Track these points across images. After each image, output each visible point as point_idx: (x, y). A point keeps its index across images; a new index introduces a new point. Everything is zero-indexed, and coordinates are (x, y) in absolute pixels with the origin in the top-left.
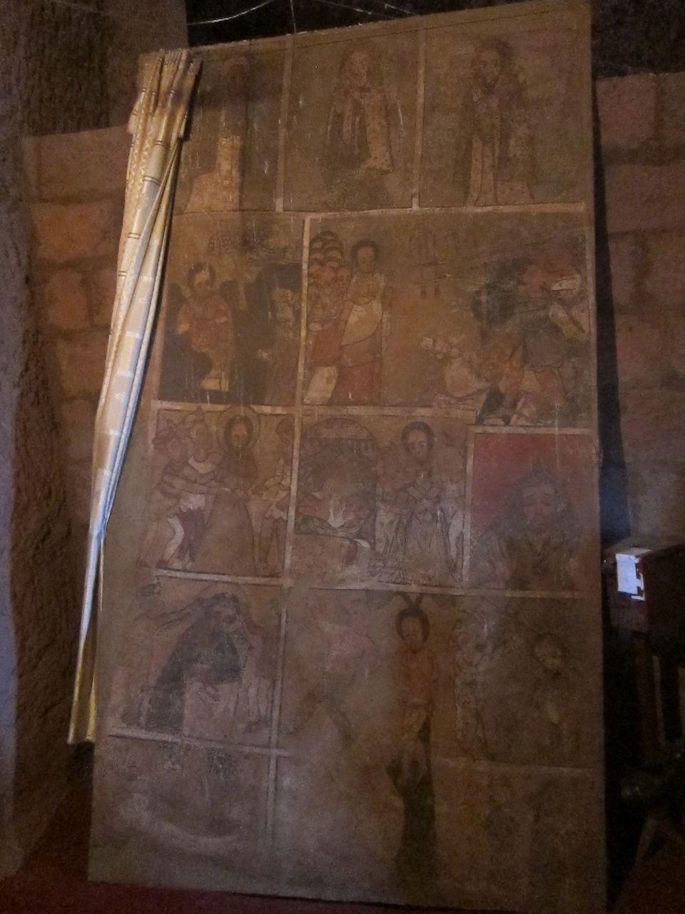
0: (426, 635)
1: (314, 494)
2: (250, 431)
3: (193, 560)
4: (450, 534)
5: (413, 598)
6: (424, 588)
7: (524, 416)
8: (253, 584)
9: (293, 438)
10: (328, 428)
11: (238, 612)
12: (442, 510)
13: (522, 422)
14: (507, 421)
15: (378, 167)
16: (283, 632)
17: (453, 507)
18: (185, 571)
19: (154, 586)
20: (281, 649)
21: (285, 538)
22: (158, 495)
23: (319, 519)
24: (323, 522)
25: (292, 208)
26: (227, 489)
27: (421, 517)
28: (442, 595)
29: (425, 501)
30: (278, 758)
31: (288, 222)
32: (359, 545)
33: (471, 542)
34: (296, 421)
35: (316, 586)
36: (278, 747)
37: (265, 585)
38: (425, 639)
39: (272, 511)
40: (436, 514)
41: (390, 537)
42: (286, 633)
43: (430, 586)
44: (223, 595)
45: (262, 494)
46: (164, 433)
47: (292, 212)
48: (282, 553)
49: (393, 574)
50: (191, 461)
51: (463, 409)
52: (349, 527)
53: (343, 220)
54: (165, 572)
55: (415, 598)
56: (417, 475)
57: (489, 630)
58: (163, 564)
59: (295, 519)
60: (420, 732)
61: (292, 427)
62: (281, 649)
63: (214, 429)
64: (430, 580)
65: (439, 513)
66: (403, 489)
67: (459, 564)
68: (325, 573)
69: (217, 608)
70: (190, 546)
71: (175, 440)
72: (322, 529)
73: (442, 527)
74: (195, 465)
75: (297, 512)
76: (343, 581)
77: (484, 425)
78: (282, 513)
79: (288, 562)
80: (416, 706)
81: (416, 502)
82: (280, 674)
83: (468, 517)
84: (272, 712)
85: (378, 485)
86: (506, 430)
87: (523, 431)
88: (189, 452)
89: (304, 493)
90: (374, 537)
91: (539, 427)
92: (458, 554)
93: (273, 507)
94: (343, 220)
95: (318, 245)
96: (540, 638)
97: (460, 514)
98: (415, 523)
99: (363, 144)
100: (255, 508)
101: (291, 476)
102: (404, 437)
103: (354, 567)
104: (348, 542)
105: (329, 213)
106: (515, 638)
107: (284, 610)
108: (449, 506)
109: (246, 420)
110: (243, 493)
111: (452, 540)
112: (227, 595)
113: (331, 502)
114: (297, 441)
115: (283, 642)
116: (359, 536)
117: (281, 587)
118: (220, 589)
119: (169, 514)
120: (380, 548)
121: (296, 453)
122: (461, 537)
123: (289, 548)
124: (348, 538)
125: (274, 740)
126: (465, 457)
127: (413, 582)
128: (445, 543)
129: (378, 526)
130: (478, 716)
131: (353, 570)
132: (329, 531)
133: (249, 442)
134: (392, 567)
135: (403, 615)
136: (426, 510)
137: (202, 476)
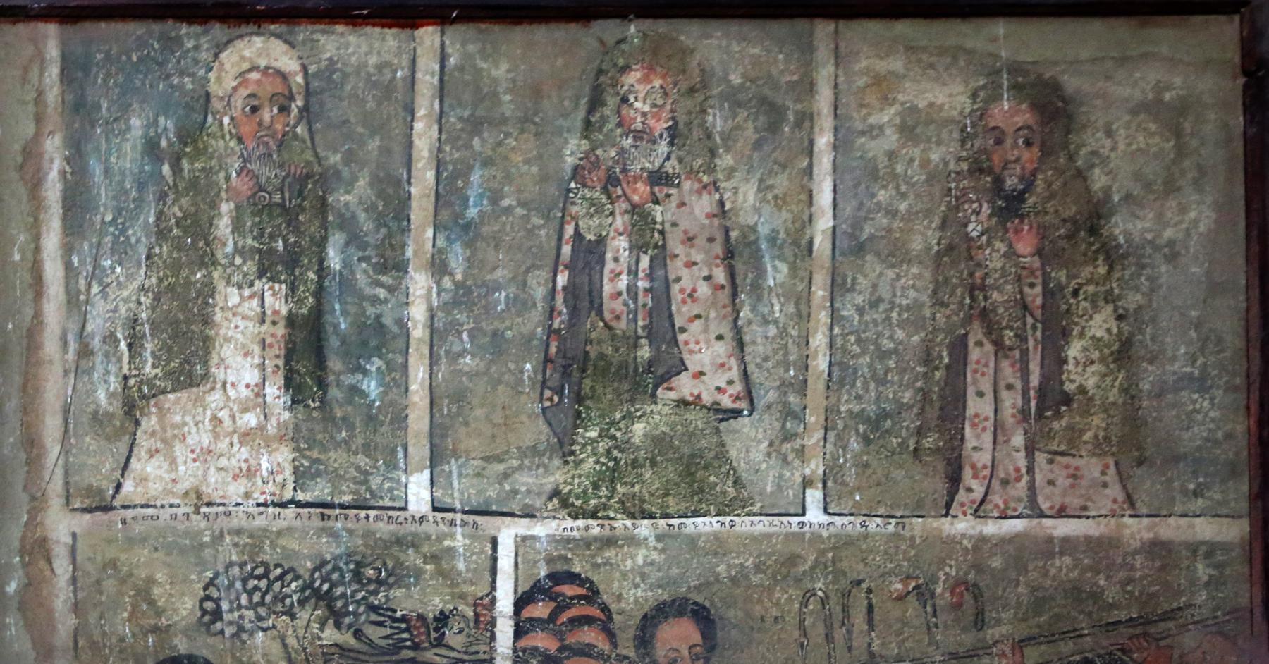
15: (707, 399)
25: (458, 506)
31: (446, 543)
47: (459, 517)
53: (609, 542)
94: (609, 542)
95: (540, 610)
99: (663, 329)
105: (569, 523)
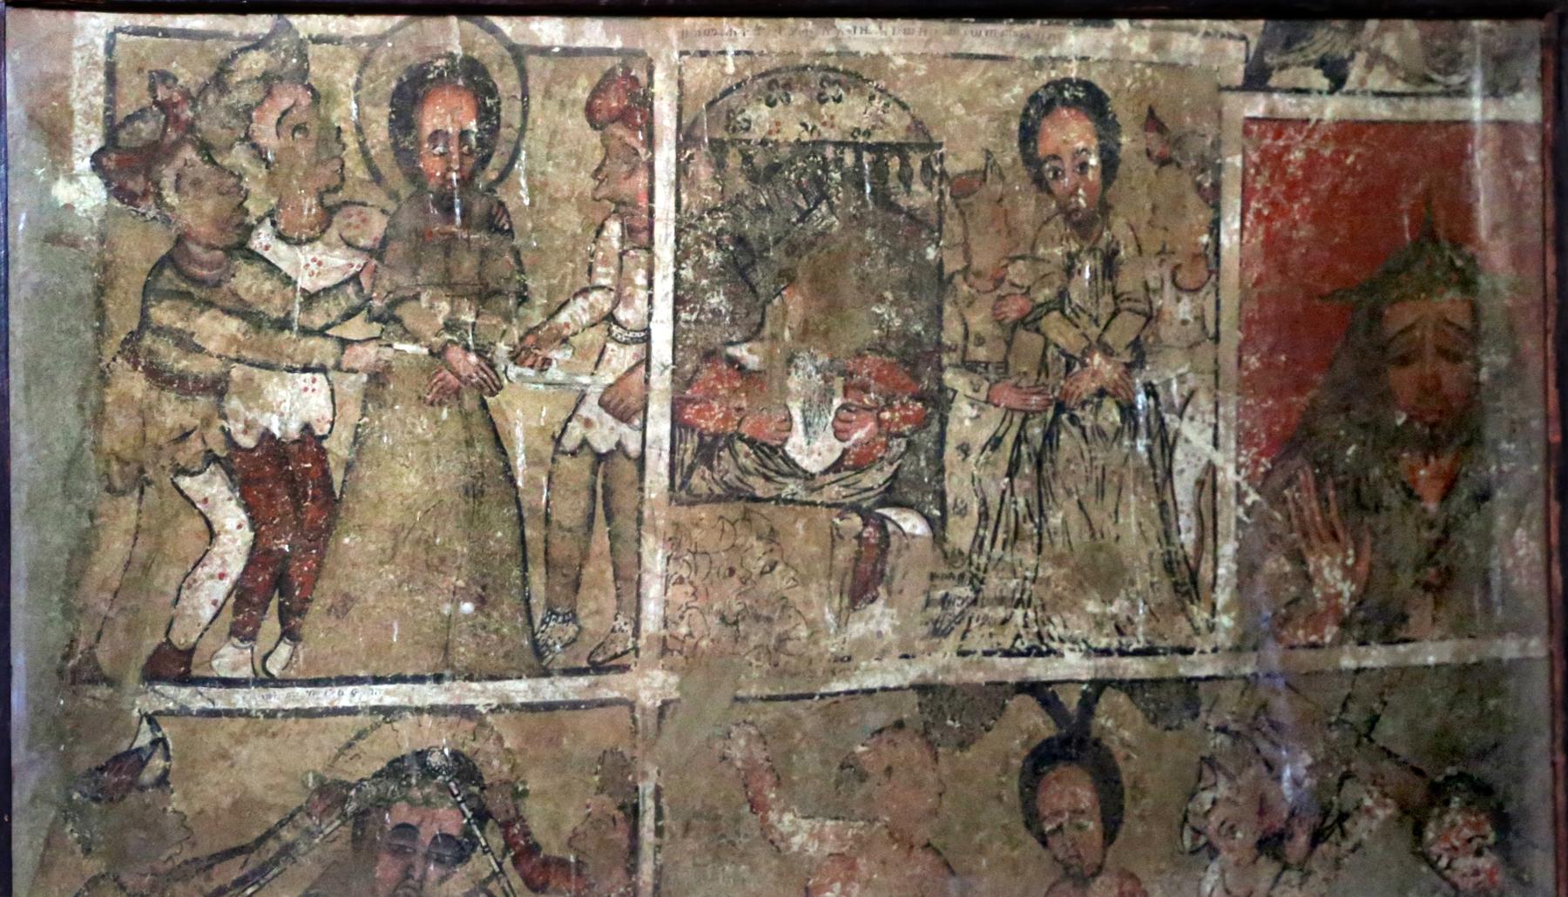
0: (1111, 825)
1: (731, 350)
2: (488, 115)
3: (290, 634)
4: (1176, 468)
5: (1071, 700)
6: (1103, 661)
7: (1387, 59)
8: (530, 708)
9: (650, 142)
10: (771, 104)
11: (482, 816)
12: (1151, 391)
13: (1378, 80)
14: (1337, 76)
17: (1181, 379)
18: (265, 681)
19: (138, 759)
21: (640, 521)
22: (135, 384)
23: (751, 442)
24: (771, 454)
26: (410, 348)
27: (1087, 417)
28: (1157, 682)
29: (1097, 359)
32: (890, 527)
33: (1240, 497)
34: (659, 75)
35: (753, 691)
37: (575, 706)
38: (1109, 836)
39: (588, 423)
40: (1133, 406)
41: (993, 499)
42: (658, 872)
43: (1123, 653)
44: (421, 755)
45: (547, 362)
46: (146, 129)
48: (628, 581)
49: (1005, 622)
50: (262, 239)
51: (1207, 34)
52: (859, 468)
54: (185, 693)
55: (1076, 698)
56: (1070, 270)
57: (1296, 783)
58: (174, 665)
59: (673, 451)
61: (645, 103)
63: (345, 111)
64: (1120, 631)
65: (1141, 399)
66: (1030, 321)
68: (783, 639)
69: (401, 813)
70: (281, 582)
71: (189, 153)
72: (768, 479)
73: (1150, 450)
74: (282, 255)
75: (677, 422)
76: (842, 663)
77: (1270, 90)
78: (624, 428)
79: (652, 611)
81: (1069, 367)
83: (1229, 409)
85: (948, 309)
86: (1332, 108)
87: (1380, 110)
88: (250, 205)
89: (701, 358)
90: (941, 496)
91: (1430, 95)
92: (1200, 541)
93: (591, 409)
96: (1438, 794)
97: (1203, 401)
98: (1067, 440)
100: (524, 413)
101: (650, 284)
102: (1028, 134)
103: (877, 608)
104: (856, 521)
106: (1368, 802)
107: (647, 787)
108: (1172, 373)
109: (474, 77)
110: (473, 358)
111: (1183, 488)
112: (434, 760)
113: (794, 382)
114: (665, 158)
116: (892, 495)
118: (405, 737)
119: (182, 459)
120: (961, 535)
121: (664, 202)
122: (1208, 480)
123: (655, 557)
124: (856, 508)
126: (1213, 197)
127: (1068, 645)
128: (1162, 505)
129: (950, 452)
131: (879, 619)
132: (792, 487)
133: (484, 161)
134: (1001, 601)
135: (1043, 758)
136: (1102, 393)
137: (310, 298)
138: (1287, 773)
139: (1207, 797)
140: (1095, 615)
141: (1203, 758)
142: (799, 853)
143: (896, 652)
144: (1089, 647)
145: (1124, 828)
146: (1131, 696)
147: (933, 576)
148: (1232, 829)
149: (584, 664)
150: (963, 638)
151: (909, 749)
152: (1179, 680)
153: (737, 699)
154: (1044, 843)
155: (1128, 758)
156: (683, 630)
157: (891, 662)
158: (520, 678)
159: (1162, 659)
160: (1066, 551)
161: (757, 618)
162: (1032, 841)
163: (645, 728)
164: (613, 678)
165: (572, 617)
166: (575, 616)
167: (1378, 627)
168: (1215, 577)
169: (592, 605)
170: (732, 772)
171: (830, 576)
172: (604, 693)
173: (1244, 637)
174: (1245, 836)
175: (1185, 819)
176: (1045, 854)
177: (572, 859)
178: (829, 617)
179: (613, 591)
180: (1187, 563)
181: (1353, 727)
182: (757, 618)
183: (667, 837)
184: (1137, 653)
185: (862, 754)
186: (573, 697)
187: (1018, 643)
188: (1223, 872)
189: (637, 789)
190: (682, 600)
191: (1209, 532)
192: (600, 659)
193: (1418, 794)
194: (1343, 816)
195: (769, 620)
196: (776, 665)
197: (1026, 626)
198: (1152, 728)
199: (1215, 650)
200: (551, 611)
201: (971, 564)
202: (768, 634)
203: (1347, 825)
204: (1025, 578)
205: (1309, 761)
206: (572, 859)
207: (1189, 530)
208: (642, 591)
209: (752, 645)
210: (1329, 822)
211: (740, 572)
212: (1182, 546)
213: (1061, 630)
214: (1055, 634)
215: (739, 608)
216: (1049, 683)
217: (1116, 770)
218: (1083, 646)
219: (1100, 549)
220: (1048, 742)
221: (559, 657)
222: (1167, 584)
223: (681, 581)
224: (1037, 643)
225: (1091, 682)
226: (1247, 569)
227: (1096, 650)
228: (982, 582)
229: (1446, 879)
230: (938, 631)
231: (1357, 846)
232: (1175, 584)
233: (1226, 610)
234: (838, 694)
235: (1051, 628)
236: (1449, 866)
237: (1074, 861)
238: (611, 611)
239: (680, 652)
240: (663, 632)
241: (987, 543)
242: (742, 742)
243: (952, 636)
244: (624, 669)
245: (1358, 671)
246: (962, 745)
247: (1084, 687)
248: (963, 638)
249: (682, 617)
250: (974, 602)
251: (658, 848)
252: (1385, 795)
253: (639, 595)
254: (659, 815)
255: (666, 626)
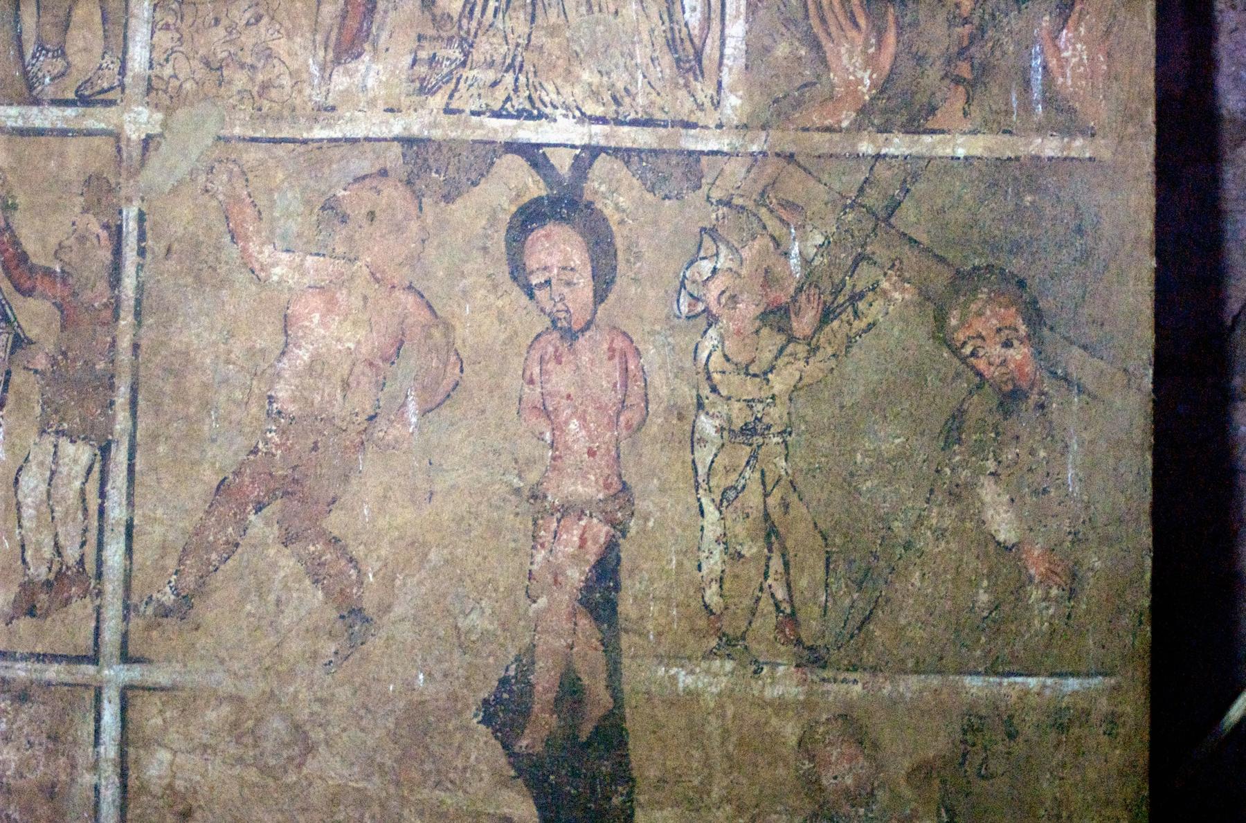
0: (603, 284)
5: (562, 162)
6: (597, 128)
8: (22, 132)
16: (129, 282)
20: (125, 343)
30: (127, 695)
35: (237, 131)
36: (126, 658)
37: (63, 133)
42: (140, 288)
43: (619, 123)
49: (495, 84)
55: (568, 161)
57: (806, 262)
60: (588, 588)
62: (125, 343)
67: (711, 50)
68: (265, 87)
79: (138, 56)
80: (567, 510)
82: (122, 420)
84: (100, 546)
92: (707, 19)
106: (885, 285)
107: (130, 213)
115: (130, 318)
117: (116, 136)
125: (110, 636)
127: (561, 111)
130: (771, 532)
134: (491, 64)
135: (530, 217)
138: (795, 250)
139: (706, 266)
140: (590, 85)
141: (703, 229)
142: (279, 283)
143: (381, 105)
144: (583, 114)
145: (616, 288)
146: (627, 163)
147: (420, 38)
148: (733, 298)
149: (71, 95)
150: (451, 96)
151: (393, 194)
152: (681, 152)
153: (219, 138)
154: (531, 296)
155: (622, 222)
156: (168, 71)
157: (378, 115)
158: (11, 104)
159: (662, 131)
160: (561, 21)
161: (242, 66)
162: (517, 293)
163: (130, 157)
164: (98, 110)
165: (61, 52)
166: (64, 53)
167: (901, 118)
168: (722, 56)
169: (81, 44)
170: (214, 203)
171: (315, 32)
172: (90, 123)
173: (751, 115)
174: (748, 309)
175: (683, 285)
176: (532, 306)
177: (58, 270)
178: (315, 70)
179: (101, 33)
180: (691, 41)
181: (870, 211)
182: (242, 66)
183: (149, 256)
184: (634, 123)
185: (344, 197)
186: (59, 125)
187: (508, 105)
188: (722, 339)
189: (120, 212)
190: (170, 45)
191: (716, 16)
192: (87, 93)
193: (940, 279)
194: (855, 298)
195: (253, 67)
196: (260, 110)
197: (516, 90)
198: (649, 197)
199: (720, 126)
200: (41, 47)
201: (460, 27)
202: (252, 79)
203: (861, 305)
204: (518, 45)
205: (819, 240)
206: (58, 270)
207: (694, 9)
208: (130, 34)
209: (235, 89)
210: (841, 300)
211: (225, 22)
212: (686, 25)
213: (554, 96)
214: (546, 99)
215: (226, 54)
216: (539, 146)
217: (611, 234)
218: (578, 114)
219: (598, 23)
220: (538, 201)
221: (47, 88)
222: (667, 60)
223: (167, 27)
224: (528, 107)
225: (584, 147)
226: (756, 52)
227: (590, 118)
228: (471, 46)
229: (973, 367)
230: (425, 89)
231: (871, 326)
232: (678, 60)
233: (733, 90)
234: (321, 140)
235: (543, 94)
236: (973, 354)
237: (562, 315)
238: (98, 50)
239: (165, 91)
240: (149, 72)
241: (478, 10)
242: (225, 177)
243: (438, 96)
244: (110, 103)
245: (878, 157)
246: (448, 198)
247: (578, 152)
248: (451, 96)
249: (167, 60)
250: (464, 64)
251: (140, 267)
252: (904, 280)
253: (125, 38)
254: (142, 236)
255: (151, 67)
